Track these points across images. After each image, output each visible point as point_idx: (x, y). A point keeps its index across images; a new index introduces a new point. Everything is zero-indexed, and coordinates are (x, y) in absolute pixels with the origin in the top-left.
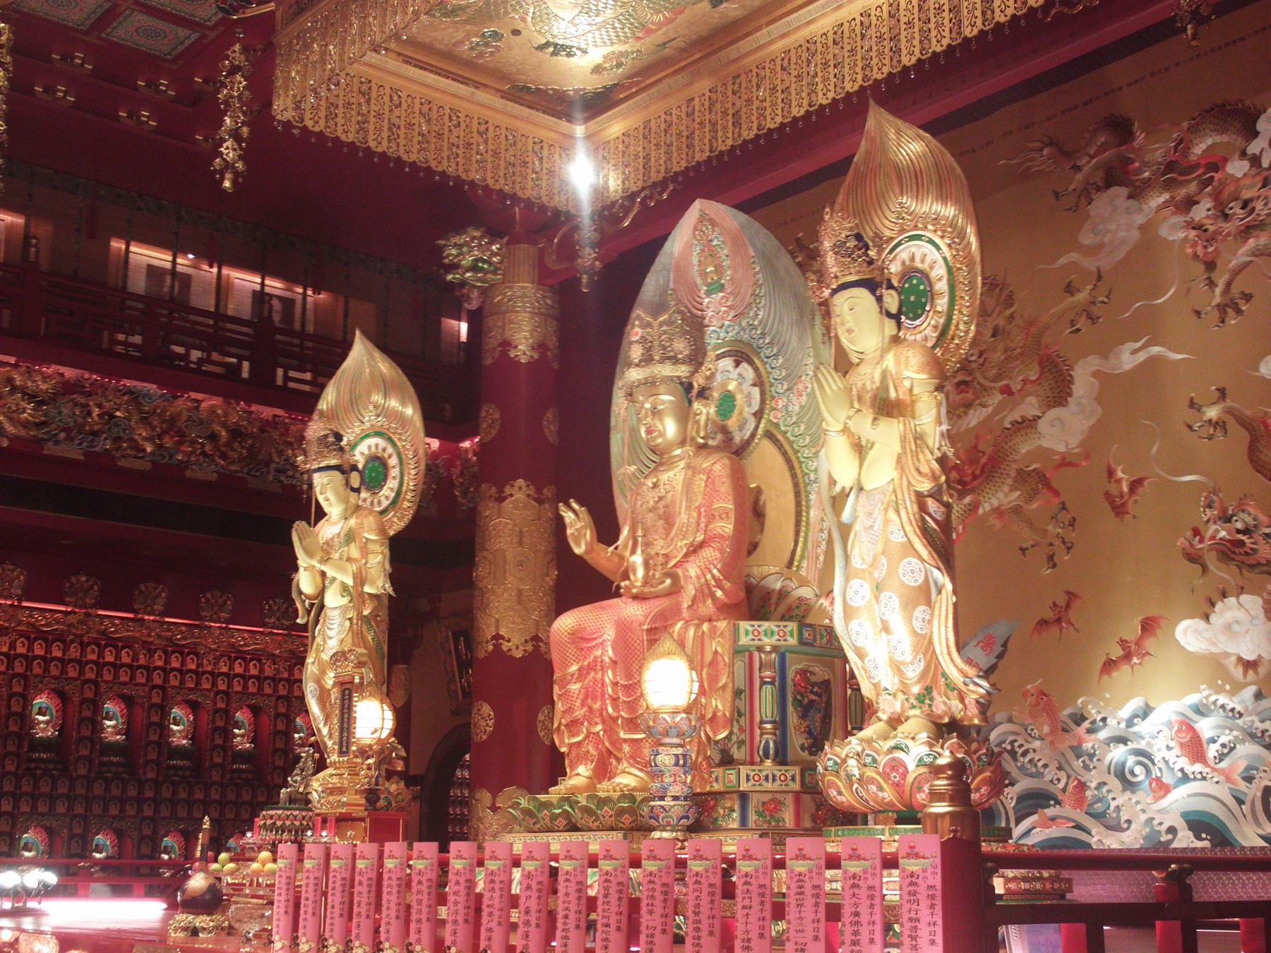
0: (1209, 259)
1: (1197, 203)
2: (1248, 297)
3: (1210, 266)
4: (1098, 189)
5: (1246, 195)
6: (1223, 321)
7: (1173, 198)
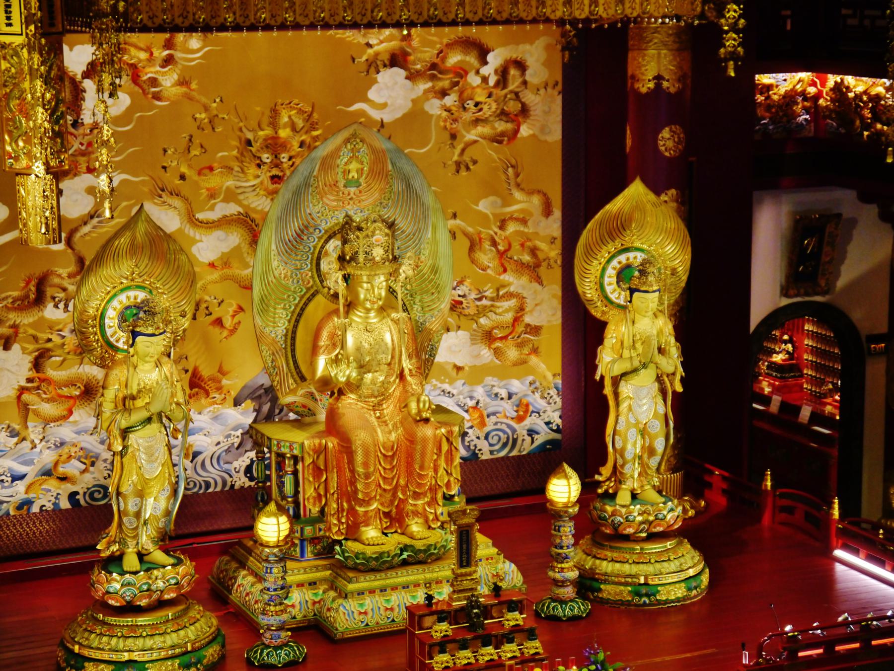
0: (453, 132)
1: (449, 95)
2: (475, 162)
3: (453, 136)
4: (385, 66)
5: (478, 99)
6: (458, 172)
7: (433, 87)
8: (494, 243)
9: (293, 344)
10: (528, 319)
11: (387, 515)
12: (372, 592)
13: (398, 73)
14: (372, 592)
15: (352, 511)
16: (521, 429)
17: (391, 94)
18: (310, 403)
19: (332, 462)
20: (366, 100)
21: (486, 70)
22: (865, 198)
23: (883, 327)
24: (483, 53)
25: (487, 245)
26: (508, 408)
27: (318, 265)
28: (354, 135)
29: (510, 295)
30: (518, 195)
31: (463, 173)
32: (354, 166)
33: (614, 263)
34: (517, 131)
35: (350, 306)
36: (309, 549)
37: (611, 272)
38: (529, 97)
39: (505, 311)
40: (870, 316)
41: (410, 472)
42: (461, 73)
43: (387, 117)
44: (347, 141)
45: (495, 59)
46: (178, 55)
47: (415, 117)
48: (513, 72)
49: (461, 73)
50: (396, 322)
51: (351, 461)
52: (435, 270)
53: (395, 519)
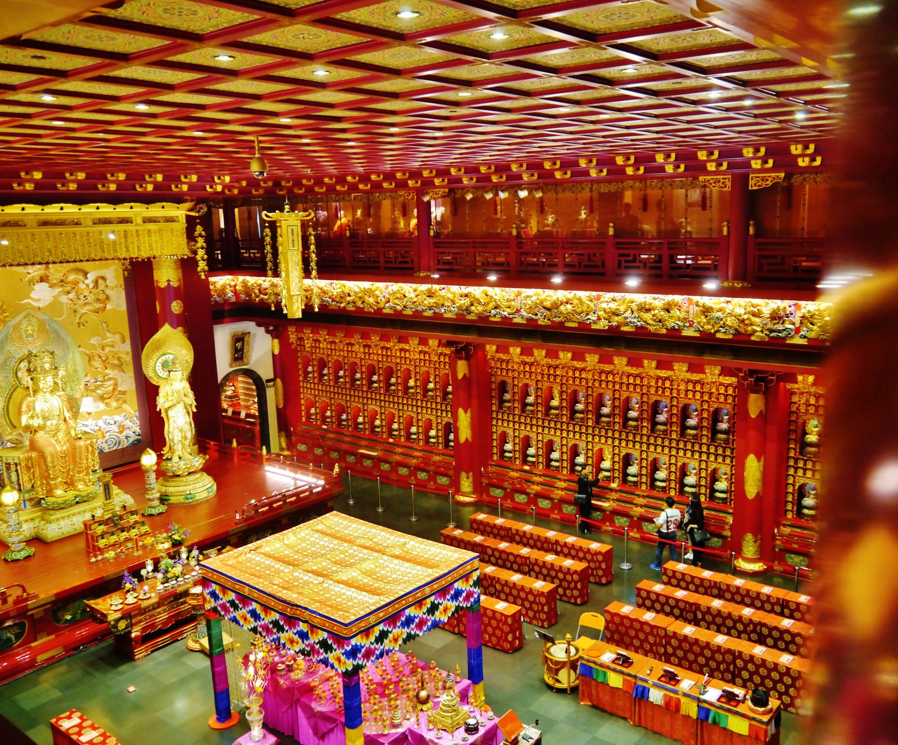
3: (75, 311)
8: (100, 357)
9: (8, 412)
10: (119, 389)
11: (66, 483)
12: (63, 518)
13: (44, 285)
14: (63, 518)
15: (48, 484)
16: (122, 436)
17: (42, 295)
18: (20, 438)
19: (35, 463)
20: (30, 298)
21: (87, 282)
22: (259, 325)
23: (272, 377)
24: (86, 274)
25: (96, 358)
26: (115, 428)
27: (16, 374)
28: (29, 314)
29: (111, 379)
30: (109, 335)
31: (82, 327)
32: (30, 328)
33: (160, 360)
34: (105, 307)
35: (35, 392)
36: (28, 504)
37: (159, 364)
38: (109, 292)
39: (109, 386)
40: (266, 371)
41: (75, 462)
42: (76, 283)
43: (41, 305)
44: (25, 317)
45: (91, 277)
47: (55, 305)
48: (100, 281)
49: (76, 283)
50: (60, 396)
51: (45, 461)
52: (75, 371)
53: (70, 484)
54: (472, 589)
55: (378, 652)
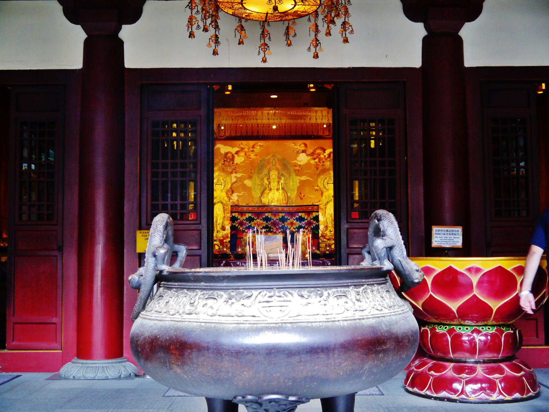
3: (317, 169)
13: (304, 154)
17: (303, 159)
20: (296, 160)
21: (325, 154)
24: (324, 151)
43: (302, 163)
46: (255, 150)
47: (308, 164)
54: (312, 221)
55: (247, 226)
